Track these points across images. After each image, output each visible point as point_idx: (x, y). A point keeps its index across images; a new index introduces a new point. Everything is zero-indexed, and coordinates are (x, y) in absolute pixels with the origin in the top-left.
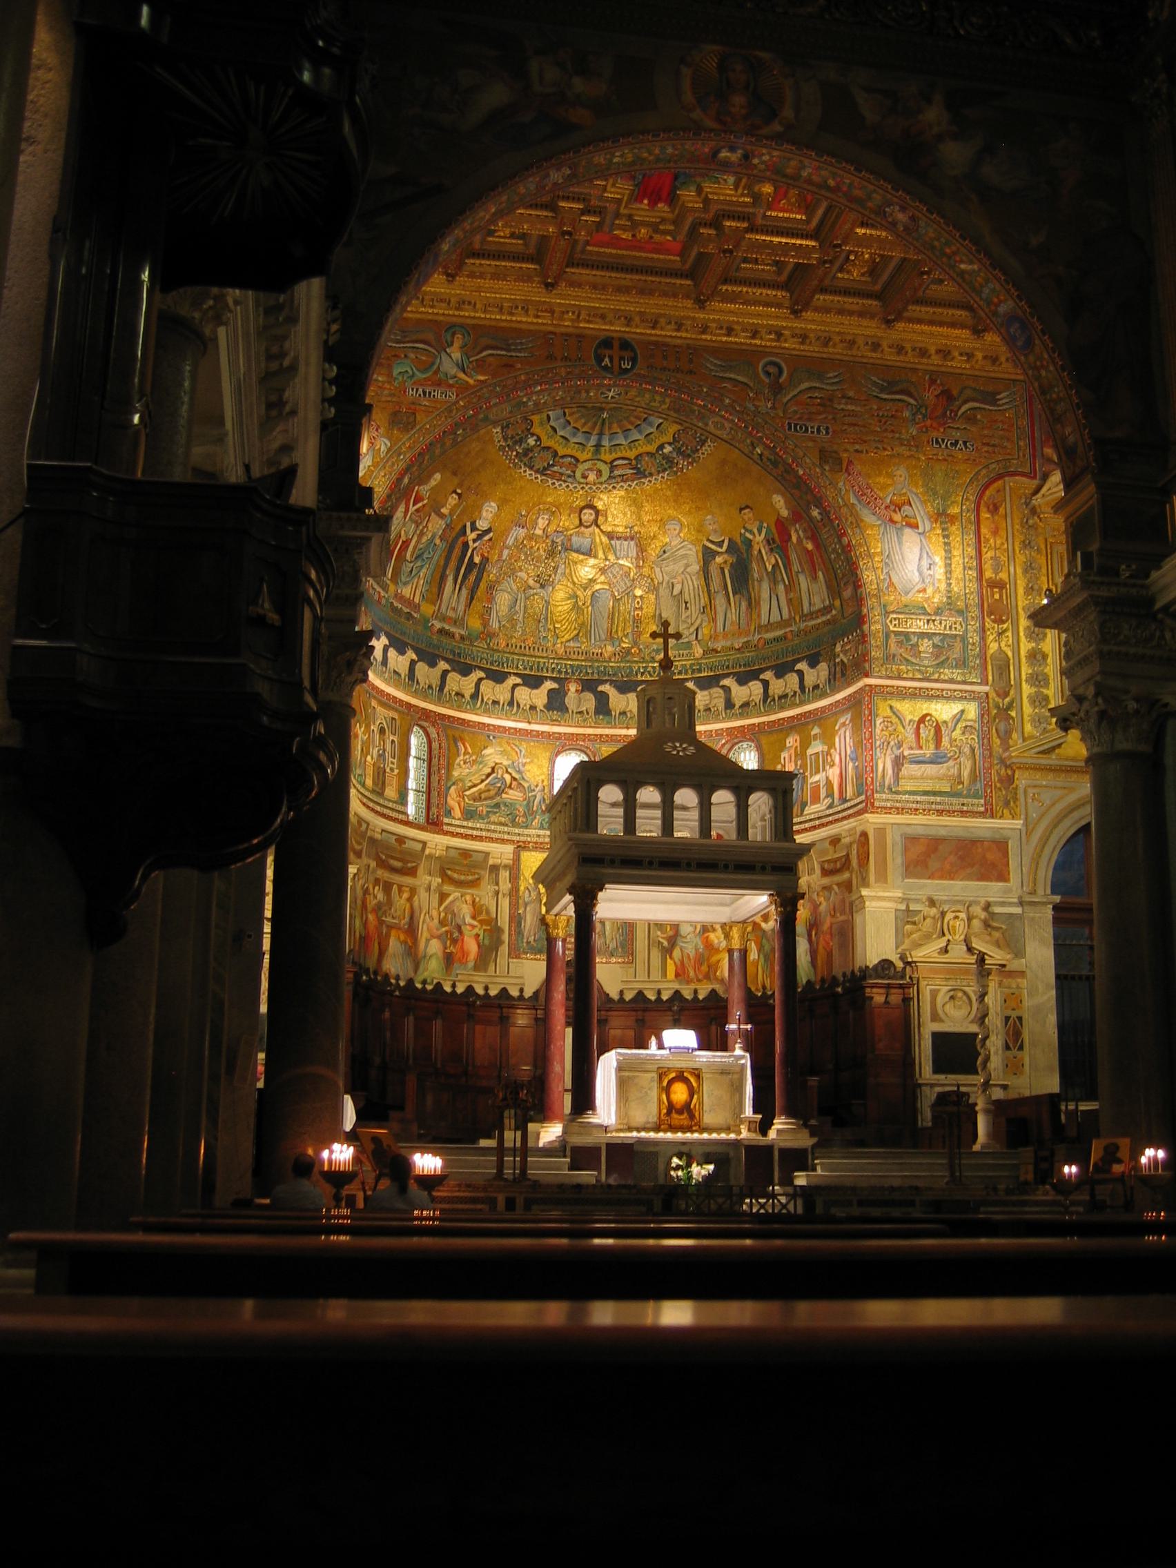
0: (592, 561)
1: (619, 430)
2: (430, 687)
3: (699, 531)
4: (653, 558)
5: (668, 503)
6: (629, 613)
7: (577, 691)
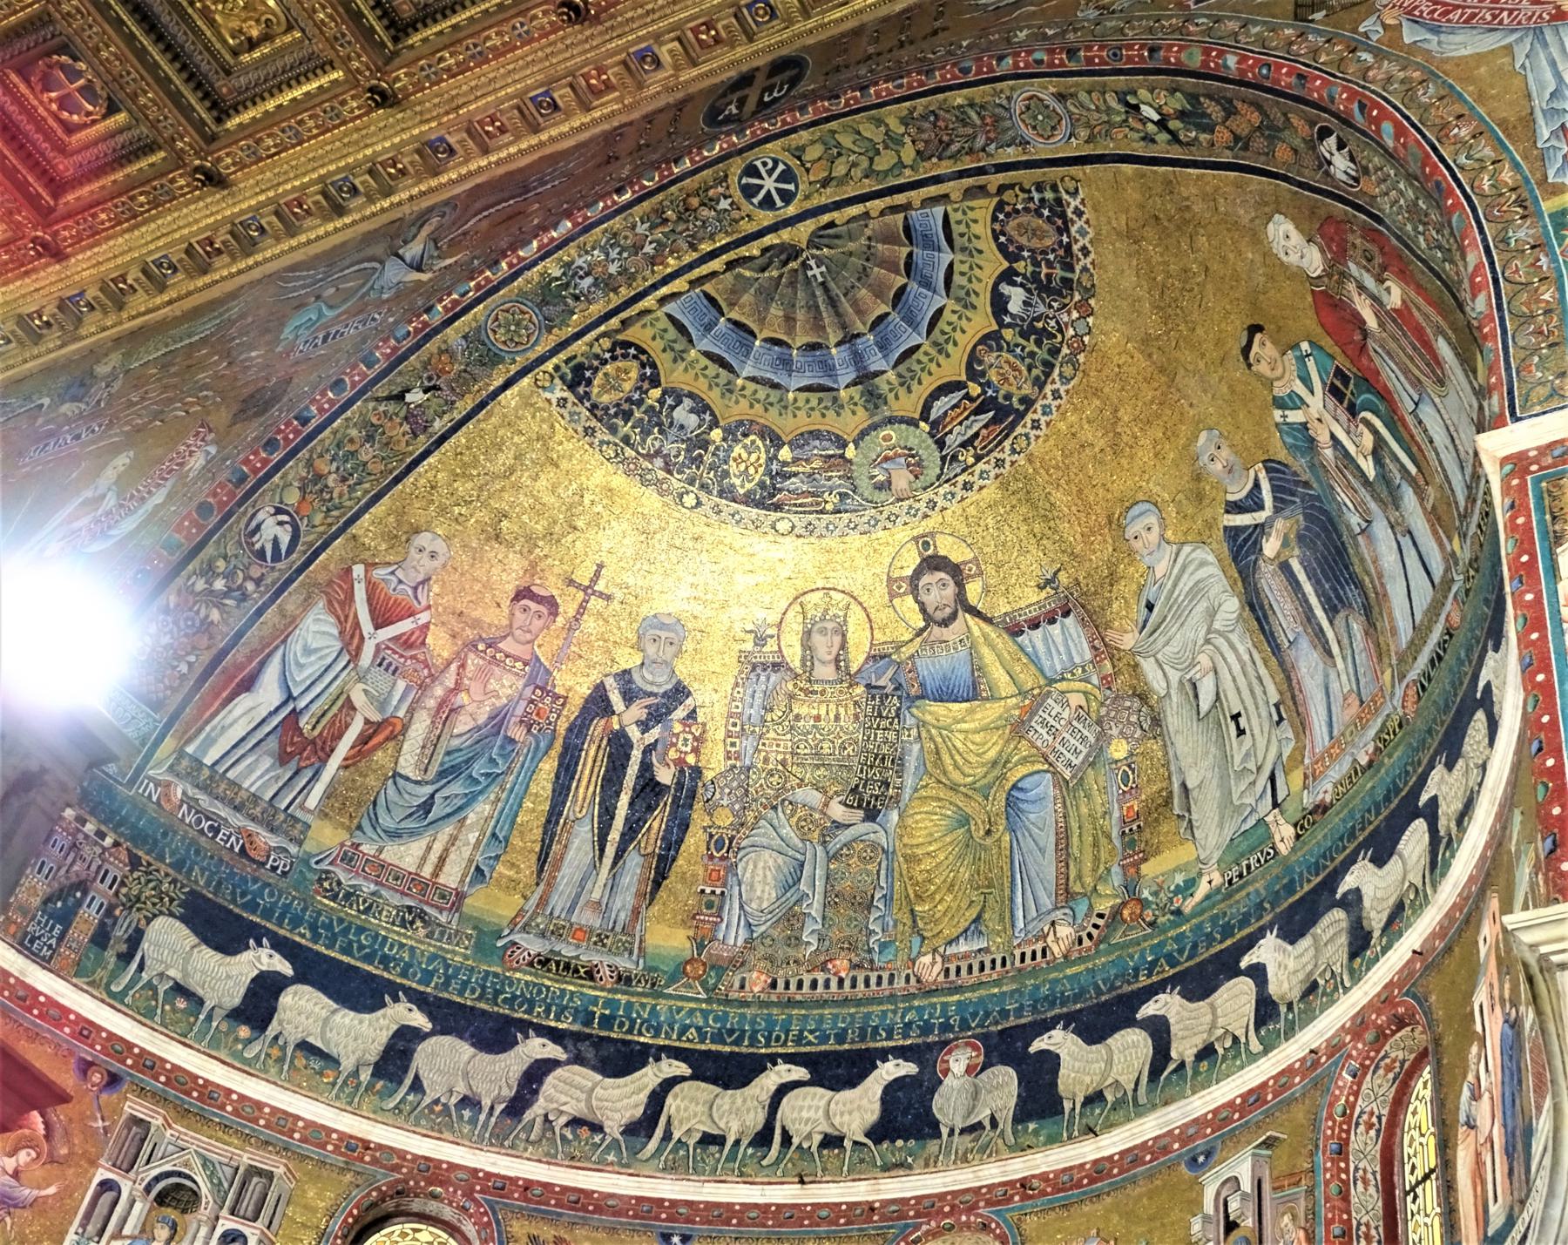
0: (990, 712)
1: (884, 309)
2: (468, 1102)
3: (1199, 497)
4: (1128, 641)
7: (969, 1070)
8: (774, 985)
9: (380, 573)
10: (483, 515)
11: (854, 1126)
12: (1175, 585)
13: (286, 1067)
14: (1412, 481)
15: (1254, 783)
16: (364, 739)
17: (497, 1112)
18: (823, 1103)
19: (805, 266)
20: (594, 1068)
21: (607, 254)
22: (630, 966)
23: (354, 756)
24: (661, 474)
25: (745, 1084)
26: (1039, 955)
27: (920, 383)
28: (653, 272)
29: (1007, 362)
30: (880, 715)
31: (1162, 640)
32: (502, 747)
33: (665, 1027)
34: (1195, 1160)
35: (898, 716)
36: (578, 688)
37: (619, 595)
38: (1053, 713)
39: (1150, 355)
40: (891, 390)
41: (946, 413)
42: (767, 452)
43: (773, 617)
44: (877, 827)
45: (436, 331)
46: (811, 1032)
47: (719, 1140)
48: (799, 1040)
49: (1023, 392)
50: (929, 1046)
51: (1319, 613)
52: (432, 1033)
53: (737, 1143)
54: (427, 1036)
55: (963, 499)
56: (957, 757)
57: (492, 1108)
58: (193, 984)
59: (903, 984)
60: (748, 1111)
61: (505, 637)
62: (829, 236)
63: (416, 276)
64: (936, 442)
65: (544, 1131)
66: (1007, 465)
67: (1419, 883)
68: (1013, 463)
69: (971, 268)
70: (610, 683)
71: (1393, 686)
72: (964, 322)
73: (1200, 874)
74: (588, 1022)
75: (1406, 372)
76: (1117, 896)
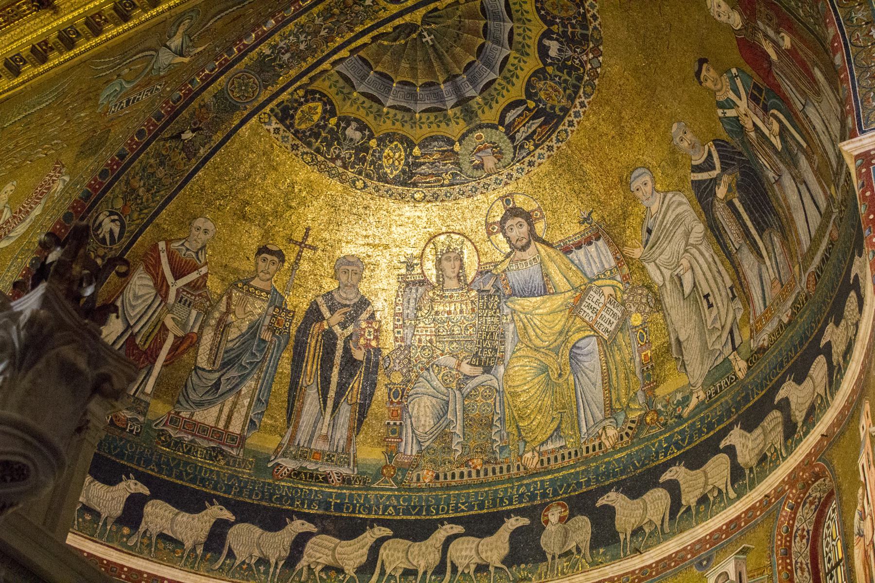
1: (472, 58)
2: (263, 561)
3: (675, 163)
4: (637, 253)
5: (614, 145)
6: (632, 359)
7: (561, 519)
8: (437, 477)
9: (175, 245)
10: (235, 205)
11: (494, 558)
12: (664, 218)
13: (153, 549)
14: (804, 152)
15: (720, 336)
16: (174, 348)
17: (280, 567)
18: (474, 546)
19: (421, 36)
20: (335, 536)
21: (298, 38)
22: (349, 472)
23: (170, 359)
24: (341, 170)
25: (426, 538)
26: (597, 447)
27: (497, 102)
28: (327, 47)
29: (551, 86)
30: (487, 307)
31: (658, 252)
32: (258, 345)
33: (374, 508)
34: (701, 563)
35: (498, 308)
36: (301, 305)
37: (321, 246)
38: (594, 300)
39: (639, 78)
40: (479, 108)
41: (514, 120)
42: (405, 151)
43: (417, 252)
44: (493, 378)
45: (198, 93)
46: (463, 504)
47: (413, 572)
48: (456, 509)
49: (562, 104)
50: (535, 507)
51: (753, 231)
52: (236, 522)
53: (425, 573)
54: (232, 525)
55: (529, 172)
56: (538, 330)
57: (277, 564)
58: (93, 504)
59: (516, 471)
60: (430, 554)
61: (253, 278)
62: (435, 17)
63: (179, 59)
64: (510, 138)
65: (309, 575)
66: (555, 149)
67: (822, 392)
68: (558, 148)
69: (524, 31)
70: (320, 300)
71: (800, 275)
72: (522, 64)
73: (691, 393)
74: (327, 508)
75: (796, 86)
76: (641, 410)
